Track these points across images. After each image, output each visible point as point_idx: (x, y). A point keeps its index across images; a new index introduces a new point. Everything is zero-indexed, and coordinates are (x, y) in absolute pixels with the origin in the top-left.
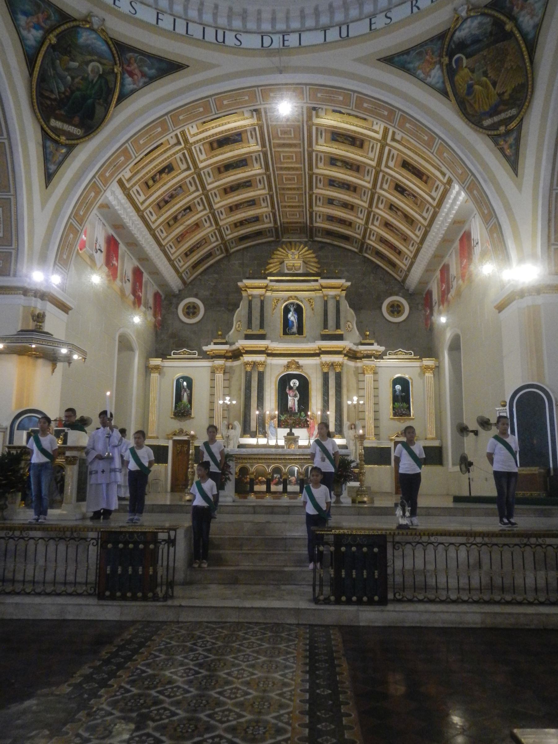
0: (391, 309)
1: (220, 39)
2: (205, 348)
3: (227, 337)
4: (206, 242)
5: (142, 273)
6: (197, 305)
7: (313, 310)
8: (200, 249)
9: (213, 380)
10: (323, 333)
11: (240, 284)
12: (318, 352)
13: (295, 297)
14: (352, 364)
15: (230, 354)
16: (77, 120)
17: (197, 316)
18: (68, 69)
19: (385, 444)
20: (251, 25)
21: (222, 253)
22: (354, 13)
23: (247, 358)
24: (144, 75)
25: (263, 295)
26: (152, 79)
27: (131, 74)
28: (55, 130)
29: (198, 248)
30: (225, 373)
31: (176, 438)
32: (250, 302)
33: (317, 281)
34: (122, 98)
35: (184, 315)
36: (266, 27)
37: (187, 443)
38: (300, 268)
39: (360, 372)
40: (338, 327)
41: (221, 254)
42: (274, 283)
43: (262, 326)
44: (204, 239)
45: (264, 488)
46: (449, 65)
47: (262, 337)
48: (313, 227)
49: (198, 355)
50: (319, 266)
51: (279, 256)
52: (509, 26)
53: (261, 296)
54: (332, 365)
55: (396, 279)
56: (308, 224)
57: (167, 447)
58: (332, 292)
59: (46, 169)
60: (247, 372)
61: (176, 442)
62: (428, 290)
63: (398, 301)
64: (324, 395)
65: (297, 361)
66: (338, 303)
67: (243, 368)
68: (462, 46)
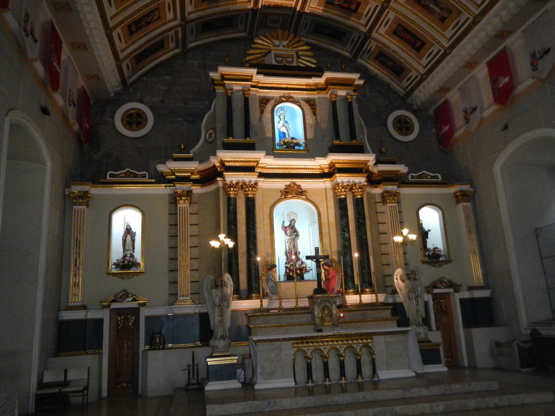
0: (398, 125)
2: (161, 168)
3: (192, 151)
4: (159, 18)
5: (62, 42)
6: (144, 113)
7: (315, 114)
8: (151, 27)
9: (174, 214)
11: (212, 74)
12: (326, 171)
13: (291, 97)
15: (197, 177)
17: (143, 127)
21: (177, 47)
23: (231, 177)
29: (148, 23)
30: (191, 203)
31: (115, 306)
33: (320, 76)
35: (124, 125)
37: (135, 311)
38: (292, 62)
39: (377, 201)
40: (353, 135)
41: (174, 49)
43: (247, 134)
44: (158, 8)
47: (251, 147)
48: (304, 13)
49: (149, 178)
50: (315, 62)
51: (260, 46)
53: (243, 91)
54: (351, 187)
55: (395, 93)
56: (298, 8)
57: (100, 322)
58: (342, 93)
60: (229, 199)
62: (446, 99)
63: (405, 116)
64: (343, 230)
65: (298, 183)
66: (350, 105)
67: (221, 193)
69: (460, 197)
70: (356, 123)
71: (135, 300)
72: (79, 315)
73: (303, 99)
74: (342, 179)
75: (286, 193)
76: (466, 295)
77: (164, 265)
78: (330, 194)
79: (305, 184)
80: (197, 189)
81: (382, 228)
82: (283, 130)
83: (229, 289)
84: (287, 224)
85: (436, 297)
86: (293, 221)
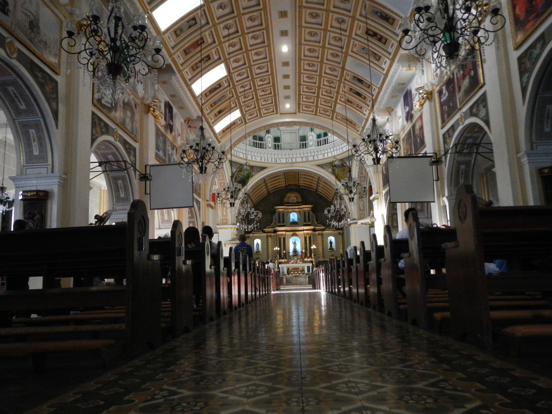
2: (264, 230)
9: (267, 240)
11: (275, 207)
14: (314, 233)
18: (241, 175)
20: (284, 157)
22: (309, 154)
26: (259, 172)
32: (279, 214)
33: (301, 205)
34: (252, 176)
36: (287, 157)
43: (283, 222)
45: (293, 273)
46: (333, 169)
52: (345, 165)
53: (283, 211)
54: (308, 234)
68: (335, 166)
69: (339, 233)
70: (311, 216)
74: (305, 232)
75: (293, 235)
77: (266, 252)
79: (297, 233)
80: (272, 234)
81: (318, 242)
83: (278, 257)
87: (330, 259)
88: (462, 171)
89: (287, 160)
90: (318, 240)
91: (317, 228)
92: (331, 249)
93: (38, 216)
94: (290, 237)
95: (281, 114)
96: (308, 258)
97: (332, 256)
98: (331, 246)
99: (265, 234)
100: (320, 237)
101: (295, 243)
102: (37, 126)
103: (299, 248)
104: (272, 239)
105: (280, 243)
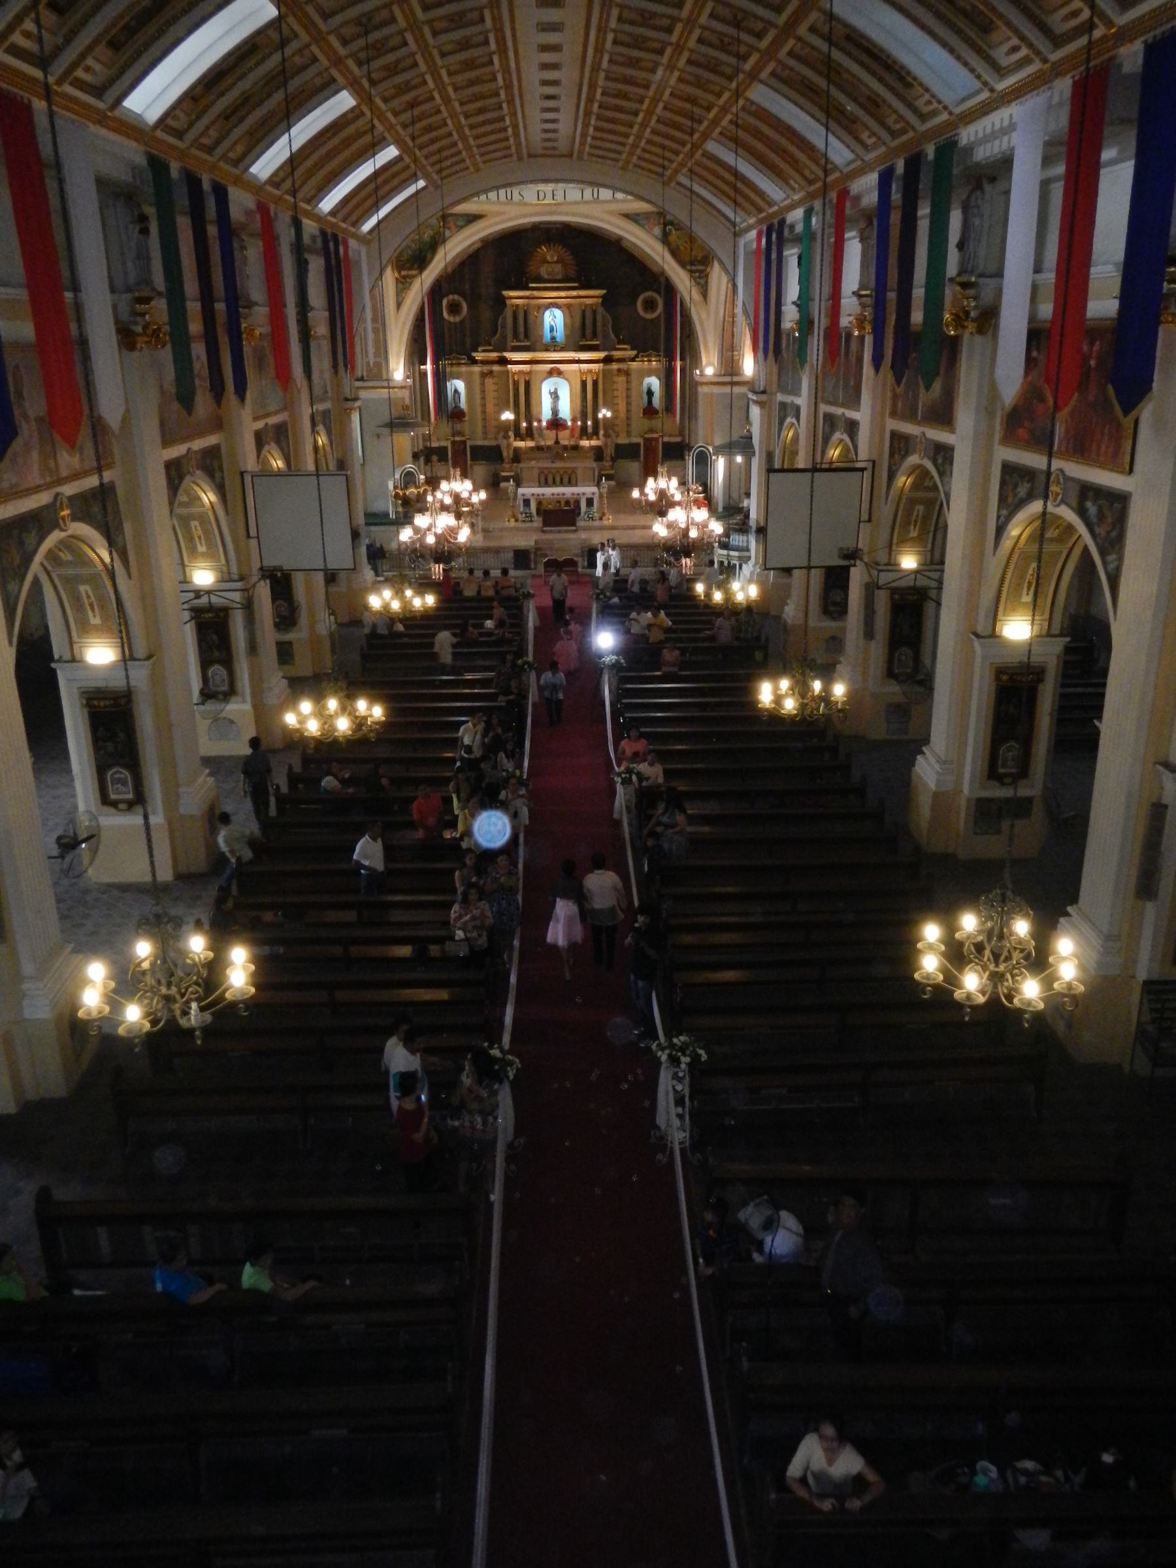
1: (509, 197)
2: (474, 354)
7: (572, 316)
10: (581, 343)
11: (506, 293)
14: (609, 367)
16: (416, 266)
19: (635, 440)
24: (457, 226)
25: (528, 305)
26: (462, 227)
27: (449, 228)
28: (405, 277)
34: (444, 241)
37: (464, 442)
42: (536, 293)
43: (527, 336)
46: (664, 230)
53: (524, 305)
54: (590, 371)
59: (397, 301)
60: (514, 381)
61: (453, 443)
66: (594, 312)
68: (671, 223)
71: (463, 436)
72: (435, 444)
73: (564, 305)
75: (551, 373)
76: (666, 439)
78: (578, 374)
79: (562, 367)
80: (496, 368)
81: (616, 394)
82: (552, 323)
83: (512, 439)
84: (552, 391)
85: (646, 440)
86: (556, 389)
87: (646, 440)
88: (917, 516)
89: (541, 197)
90: (615, 387)
91: (617, 354)
92: (650, 411)
93: (122, 736)
94: (545, 379)
95: (530, 156)
96: (589, 438)
97: (651, 431)
98: (650, 402)
99: (476, 369)
100: (621, 379)
101: (555, 396)
102: (93, 580)
103: (565, 411)
104: (495, 380)
105: (516, 395)
